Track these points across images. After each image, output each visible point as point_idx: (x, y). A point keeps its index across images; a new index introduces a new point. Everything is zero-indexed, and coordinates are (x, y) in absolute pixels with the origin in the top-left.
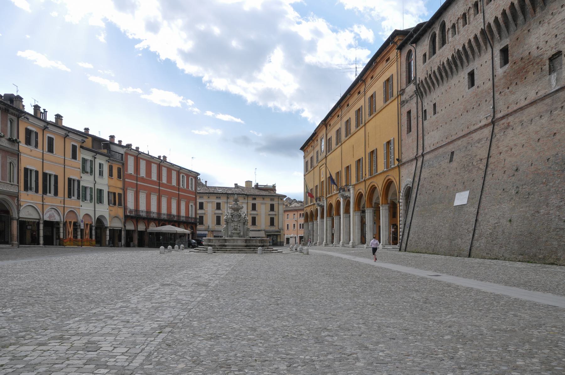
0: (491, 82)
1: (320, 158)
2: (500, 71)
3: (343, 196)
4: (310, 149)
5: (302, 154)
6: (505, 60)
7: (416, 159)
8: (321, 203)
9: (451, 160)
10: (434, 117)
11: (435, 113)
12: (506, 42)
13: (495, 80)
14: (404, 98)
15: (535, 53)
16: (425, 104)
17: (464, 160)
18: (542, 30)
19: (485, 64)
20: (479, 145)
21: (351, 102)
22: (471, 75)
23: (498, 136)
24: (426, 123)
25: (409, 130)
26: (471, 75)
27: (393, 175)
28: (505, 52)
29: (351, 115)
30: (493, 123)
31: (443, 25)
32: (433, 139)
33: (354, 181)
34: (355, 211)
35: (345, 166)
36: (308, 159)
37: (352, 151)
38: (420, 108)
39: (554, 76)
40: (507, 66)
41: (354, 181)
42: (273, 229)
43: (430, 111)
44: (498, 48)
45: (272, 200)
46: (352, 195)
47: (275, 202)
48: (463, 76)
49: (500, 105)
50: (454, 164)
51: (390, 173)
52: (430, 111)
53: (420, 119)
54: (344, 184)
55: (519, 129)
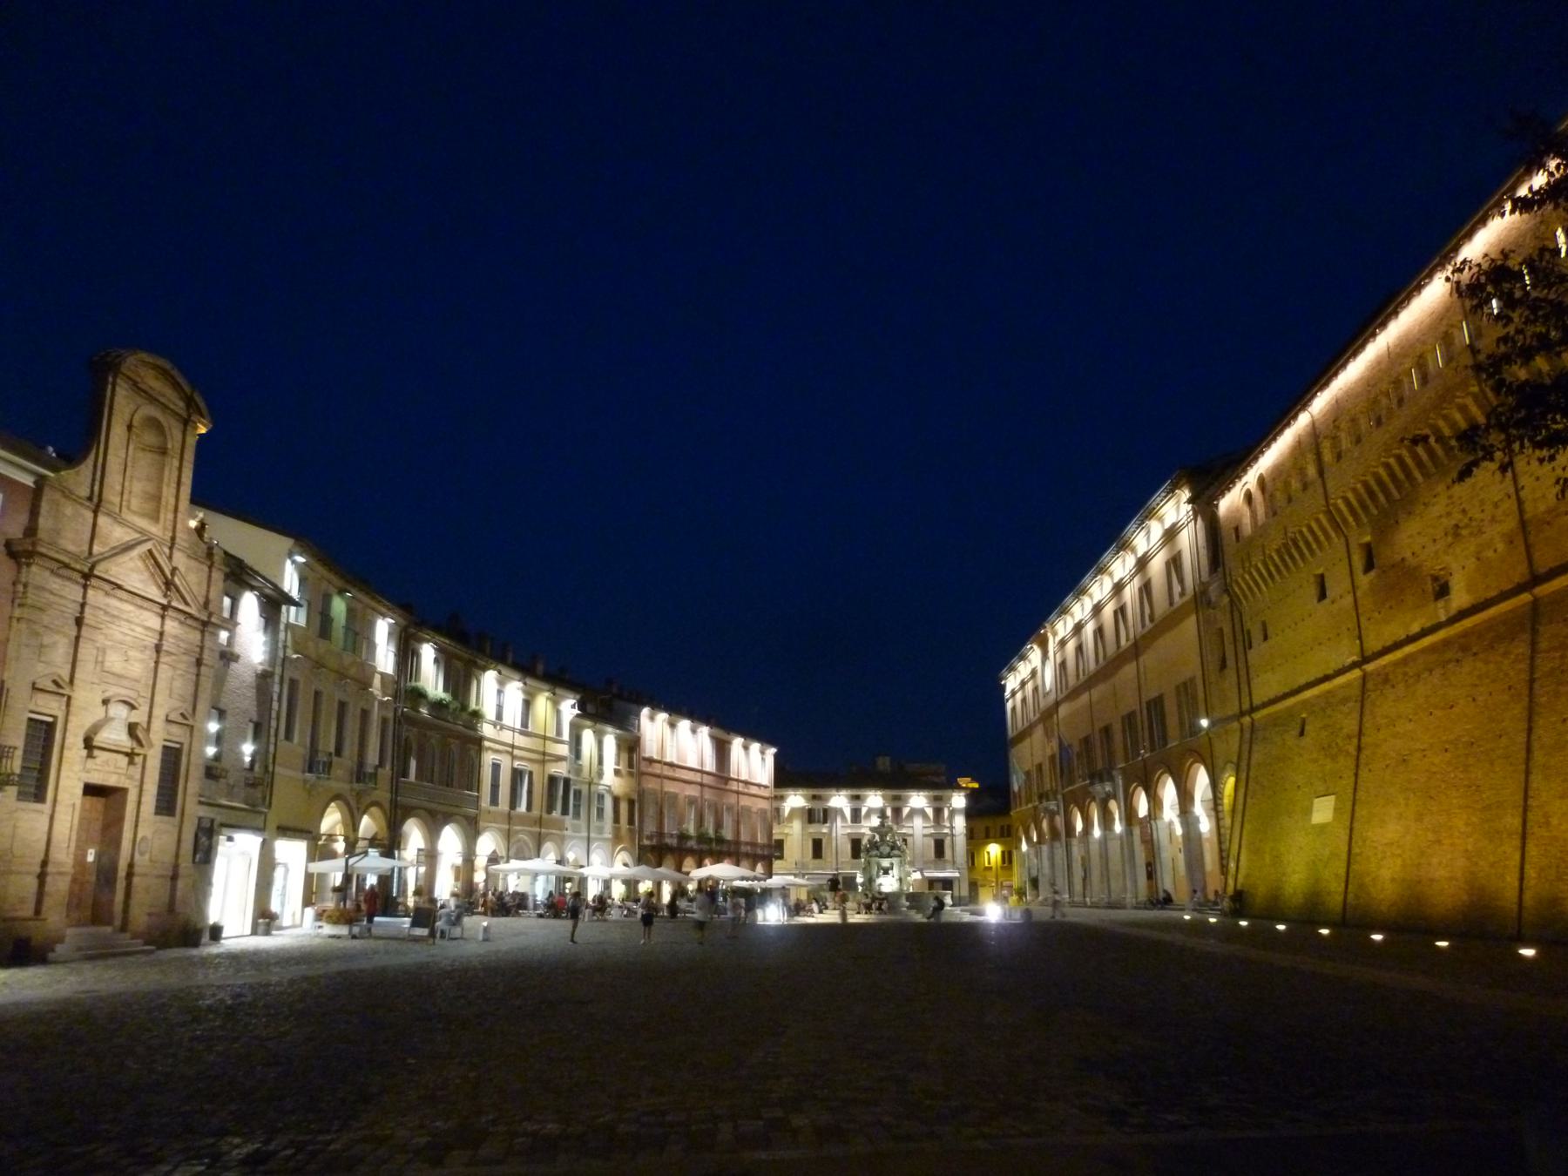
0: (1350, 598)
2: (1364, 580)
6: (1369, 566)
9: (1302, 733)
10: (1265, 645)
11: (1266, 638)
13: (1359, 594)
15: (1411, 561)
17: (1324, 734)
20: (1345, 709)
23: (1373, 696)
24: (1252, 654)
35: (1099, 725)
38: (1238, 627)
39: (1441, 604)
40: (1372, 574)
50: (1307, 741)
53: (1240, 648)
55: (1401, 686)
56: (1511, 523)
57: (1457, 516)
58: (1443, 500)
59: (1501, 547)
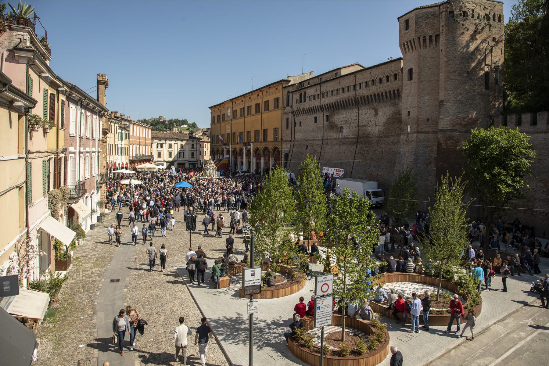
1: (226, 119)
2: (326, 123)
3: (246, 147)
4: (216, 110)
5: (210, 111)
6: (327, 120)
7: (291, 141)
8: (228, 147)
9: (307, 148)
12: (328, 114)
14: (285, 111)
15: (336, 123)
16: (296, 120)
18: (338, 117)
19: (321, 116)
21: (252, 97)
22: (316, 118)
25: (288, 127)
26: (316, 118)
27: (278, 145)
28: (327, 116)
29: (253, 104)
30: (322, 140)
31: (305, 93)
32: (298, 136)
33: (253, 140)
34: (253, 156)
36: (216, 116)
37: (252, 123)
41: (253, 140)
42: (193, 160)
43: (298, 124)
44: (325, 114)
45: (193, 141)
46: (252, 147)
47: (195, 143)
48: (311, 117)
49: (325, 135)
51: (277, 143)
52: (298, 124)
53: (293, 125)
54: (246, 141)
56: (356, 125)
57: (346, 119)
58: (345, 114)
59: (354, 128)
